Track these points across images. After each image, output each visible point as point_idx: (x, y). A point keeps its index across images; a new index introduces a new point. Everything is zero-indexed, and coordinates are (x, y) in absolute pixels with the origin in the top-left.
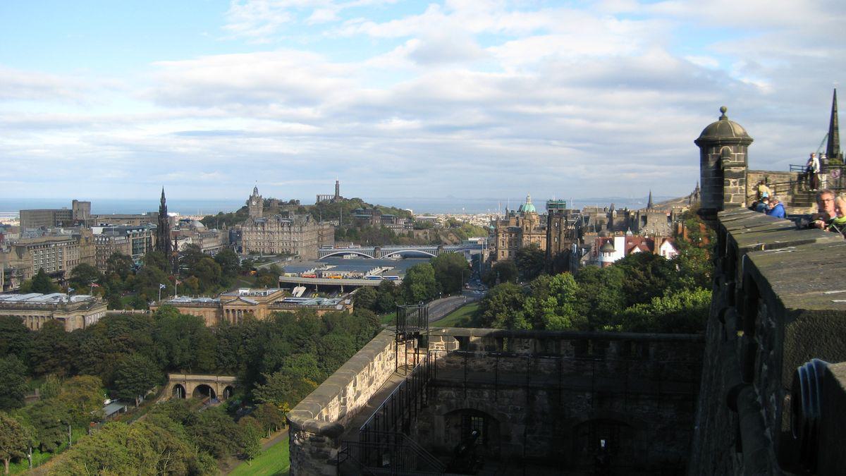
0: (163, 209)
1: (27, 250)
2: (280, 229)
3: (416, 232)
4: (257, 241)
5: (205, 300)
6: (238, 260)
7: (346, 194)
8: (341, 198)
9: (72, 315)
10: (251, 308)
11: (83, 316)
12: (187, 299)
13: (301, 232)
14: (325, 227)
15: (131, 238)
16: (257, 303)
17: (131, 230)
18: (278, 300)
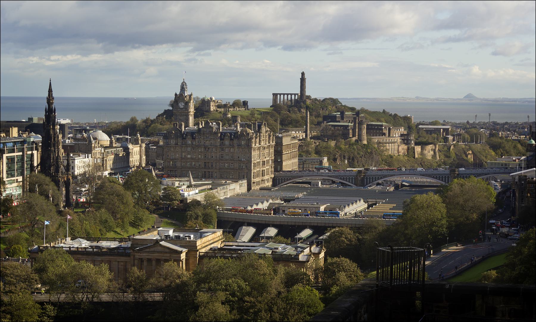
0: (50, 112)
3: (418, 149)
7: (315, 92)
8: (309, 97)
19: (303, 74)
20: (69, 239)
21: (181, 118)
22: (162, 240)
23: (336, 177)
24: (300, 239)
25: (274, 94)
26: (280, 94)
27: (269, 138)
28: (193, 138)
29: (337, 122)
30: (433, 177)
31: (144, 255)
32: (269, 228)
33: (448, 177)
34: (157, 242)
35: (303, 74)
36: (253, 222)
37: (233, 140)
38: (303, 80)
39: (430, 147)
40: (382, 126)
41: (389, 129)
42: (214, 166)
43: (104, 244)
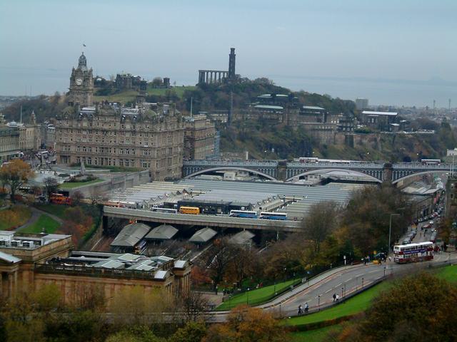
2: (118, 126)
3: (357, 138)
4: (78, 145)
7: (247, 71)
13: (153, 133)
16: (15, 260)
19: (233, 50)
21: (79, 96)
23: (254, 168)
25: (200, 71)
26: (208, 72)
27: (178, 122)
28: (90, 120)
29: (266, 104)
30: (364, 172)
33: (381, 172)
35: (233, 50)
36: (144, 220)
37: (135, 123)
38: (232, 56)
39: (370, 136)
40: (317, 110)
41: (326, 115)
42: (113, 152)
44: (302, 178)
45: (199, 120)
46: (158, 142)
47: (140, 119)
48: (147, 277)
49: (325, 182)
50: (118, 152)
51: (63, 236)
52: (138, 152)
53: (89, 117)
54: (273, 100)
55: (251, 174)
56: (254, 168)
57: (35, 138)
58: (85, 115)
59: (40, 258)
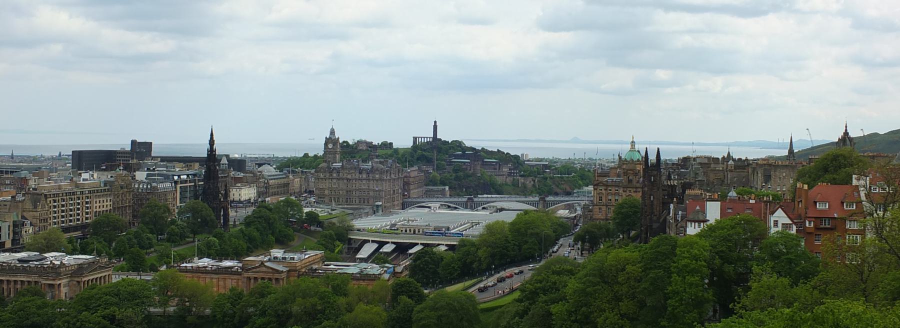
0: (211, 151)
1: (43, 198)
3: (522, 180)
5: (227, 263)
6: (301, 211)
7: (446, 135)
9: (64, 281)
10: (277, 276)
11: (78, 282)
12: (206, 262)
13: (381, 180)
14: (412, 174)
15: (178, 186)
16: (285, 269)
17: (179, 176)
18: (315, 267)
19: (435, 122)
20: (196, 258)
22: (269, 260)
23: (451, 202)
24: (411, 254)
28: (338, 172)
31: (250, 274)
32: (388, 245)
34: (262, 263)
35: (435, 122)
38: (435, 127)
39: (530, 179)
43: (227, 263)
44: (484, 208)
45: (413, 171)
46: (386, 186)
47: (372, 170)
48: (375, 278)
49: (501, 210)
50: (358, 193)
51: (318, 252)
52: (371, 193)
53: (338, 171)
54: (464, 156)
55: (449, 207)
56: (451, 202)
57: (301, 185)
58: (334, 169)
59: (302, 268)
